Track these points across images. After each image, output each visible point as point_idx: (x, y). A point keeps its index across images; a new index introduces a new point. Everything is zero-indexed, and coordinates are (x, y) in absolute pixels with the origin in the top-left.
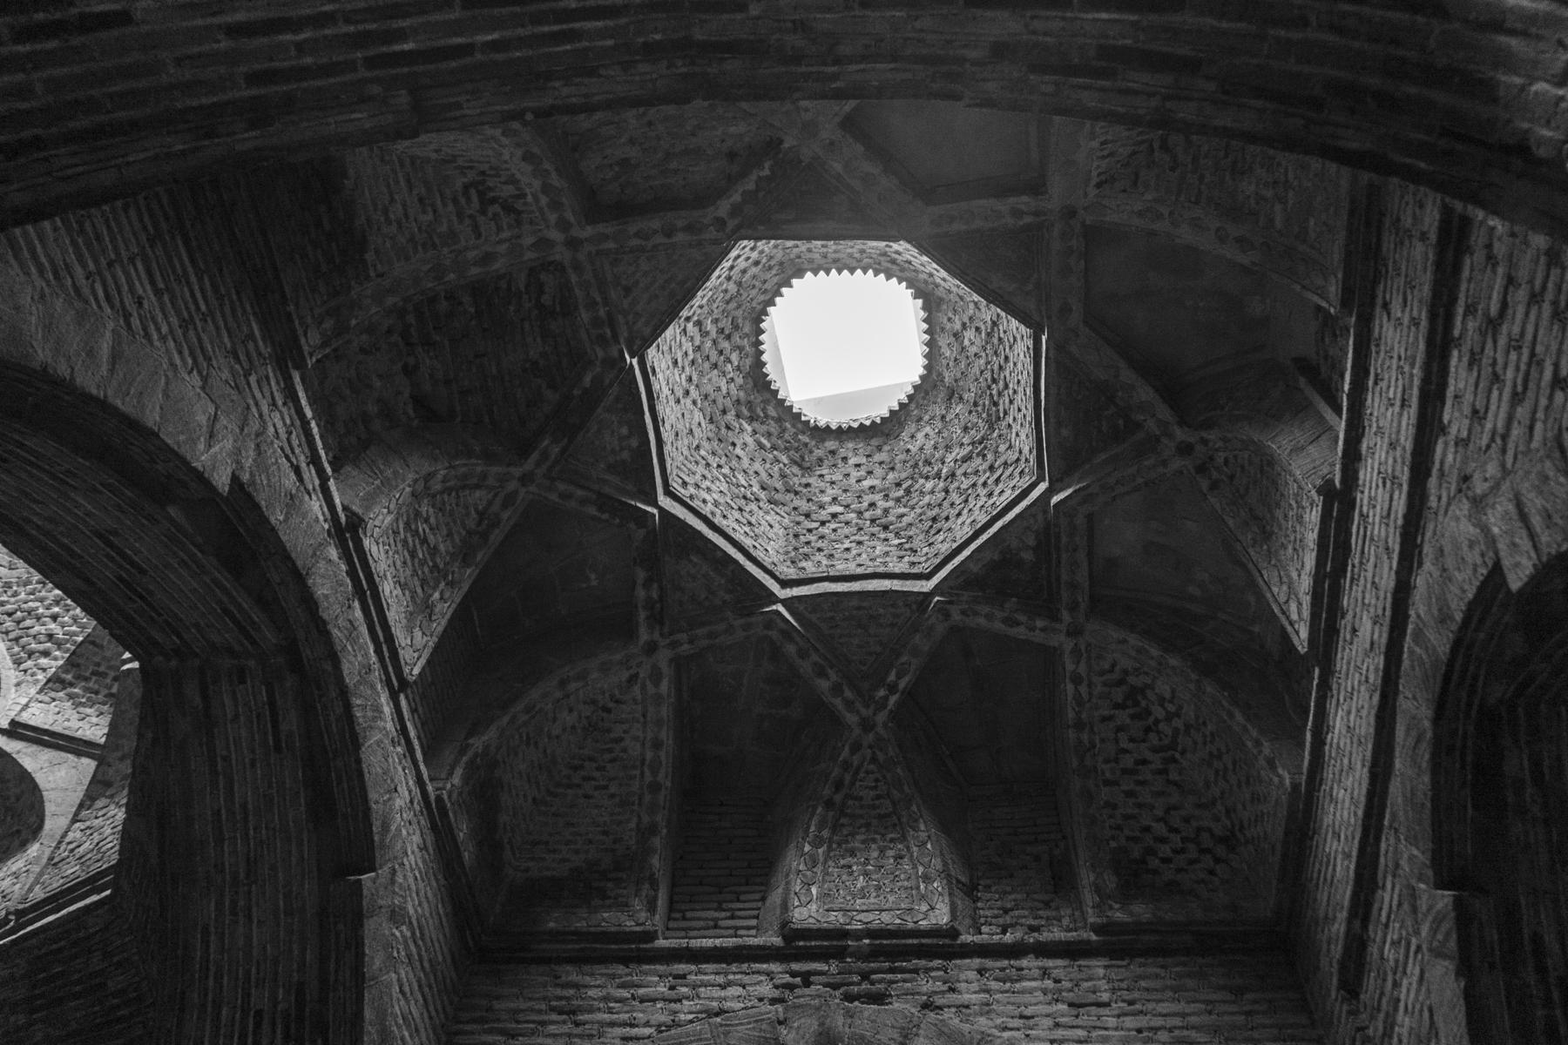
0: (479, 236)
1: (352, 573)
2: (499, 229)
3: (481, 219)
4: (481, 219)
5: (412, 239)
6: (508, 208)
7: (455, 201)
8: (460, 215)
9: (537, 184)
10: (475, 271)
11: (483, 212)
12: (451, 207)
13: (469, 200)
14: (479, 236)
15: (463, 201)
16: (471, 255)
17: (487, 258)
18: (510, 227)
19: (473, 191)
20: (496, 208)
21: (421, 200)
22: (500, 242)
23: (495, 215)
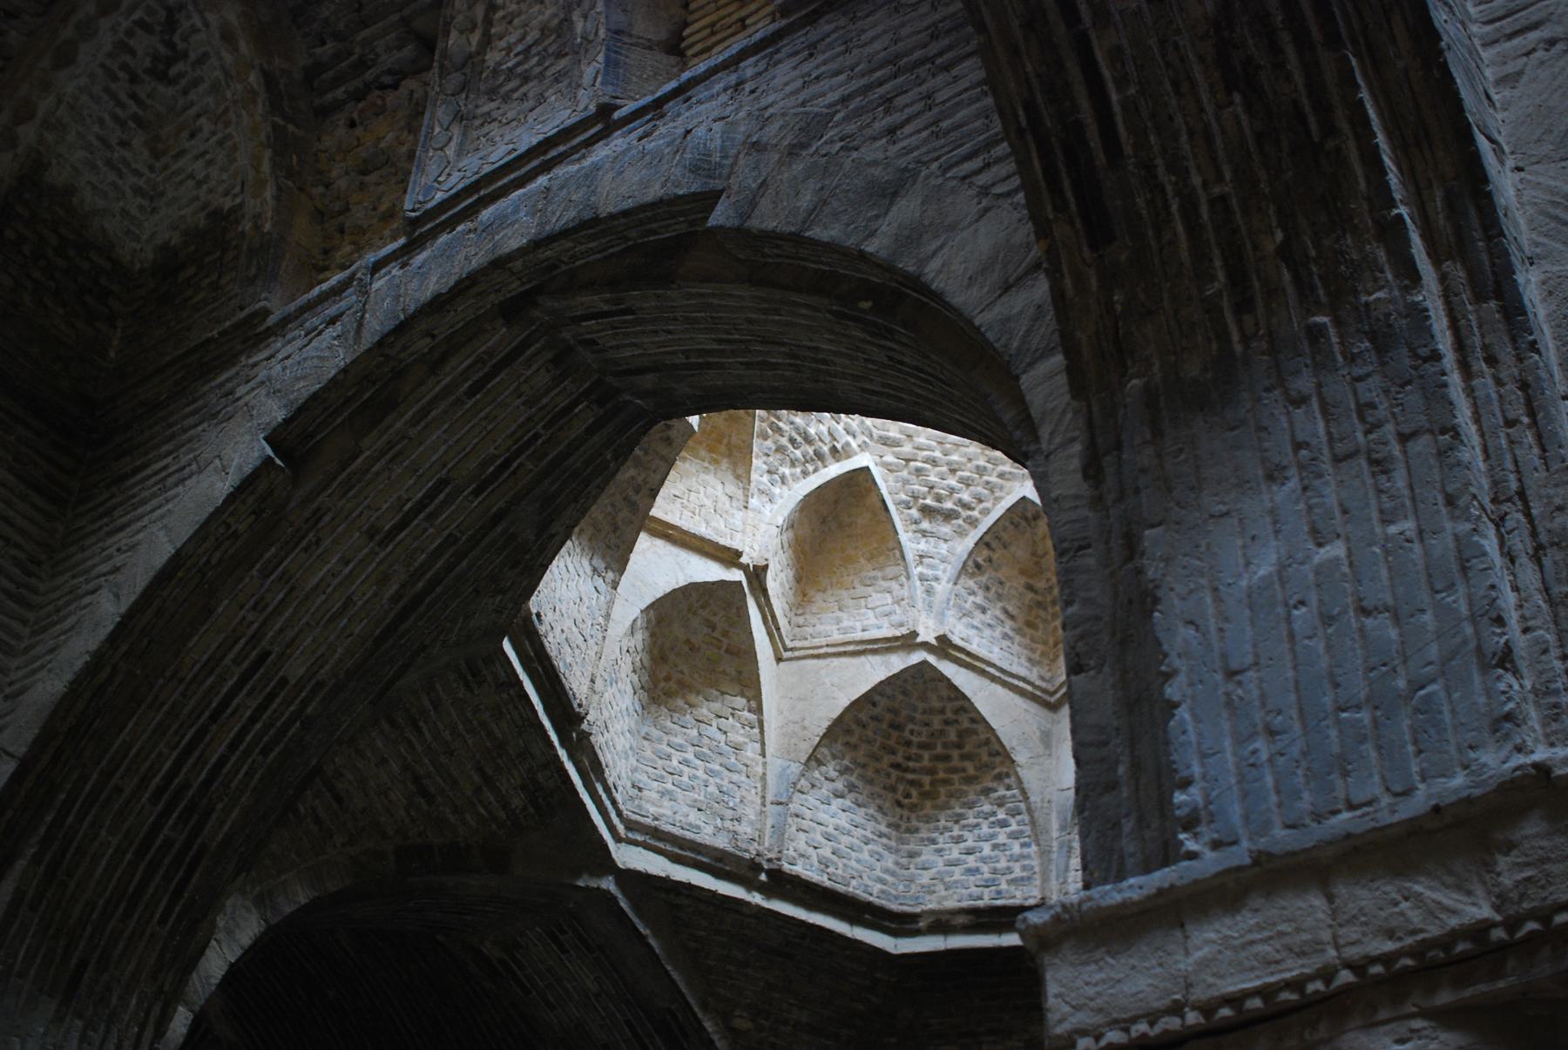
0: (206, 55)
1: (450, 225)
2: (194, 30)
3: (193, 56)
4: (193, 56)
5: (220, 143)
6: (171, 24)
7: (185, 93)
8: (196, 83)
9: (105, 24)
10: (243, 47)
11: (185, 55)
12: (192, 96)
13: (180, 75)
14: (206, 55)
15: (183, 82)
16: (228, 58)
17: (228, 37)
18: (189, 17)
19: (173, 71)
20: (176, 38)
21: (192, 136)
22: (206, 24)
23: (184, 39)
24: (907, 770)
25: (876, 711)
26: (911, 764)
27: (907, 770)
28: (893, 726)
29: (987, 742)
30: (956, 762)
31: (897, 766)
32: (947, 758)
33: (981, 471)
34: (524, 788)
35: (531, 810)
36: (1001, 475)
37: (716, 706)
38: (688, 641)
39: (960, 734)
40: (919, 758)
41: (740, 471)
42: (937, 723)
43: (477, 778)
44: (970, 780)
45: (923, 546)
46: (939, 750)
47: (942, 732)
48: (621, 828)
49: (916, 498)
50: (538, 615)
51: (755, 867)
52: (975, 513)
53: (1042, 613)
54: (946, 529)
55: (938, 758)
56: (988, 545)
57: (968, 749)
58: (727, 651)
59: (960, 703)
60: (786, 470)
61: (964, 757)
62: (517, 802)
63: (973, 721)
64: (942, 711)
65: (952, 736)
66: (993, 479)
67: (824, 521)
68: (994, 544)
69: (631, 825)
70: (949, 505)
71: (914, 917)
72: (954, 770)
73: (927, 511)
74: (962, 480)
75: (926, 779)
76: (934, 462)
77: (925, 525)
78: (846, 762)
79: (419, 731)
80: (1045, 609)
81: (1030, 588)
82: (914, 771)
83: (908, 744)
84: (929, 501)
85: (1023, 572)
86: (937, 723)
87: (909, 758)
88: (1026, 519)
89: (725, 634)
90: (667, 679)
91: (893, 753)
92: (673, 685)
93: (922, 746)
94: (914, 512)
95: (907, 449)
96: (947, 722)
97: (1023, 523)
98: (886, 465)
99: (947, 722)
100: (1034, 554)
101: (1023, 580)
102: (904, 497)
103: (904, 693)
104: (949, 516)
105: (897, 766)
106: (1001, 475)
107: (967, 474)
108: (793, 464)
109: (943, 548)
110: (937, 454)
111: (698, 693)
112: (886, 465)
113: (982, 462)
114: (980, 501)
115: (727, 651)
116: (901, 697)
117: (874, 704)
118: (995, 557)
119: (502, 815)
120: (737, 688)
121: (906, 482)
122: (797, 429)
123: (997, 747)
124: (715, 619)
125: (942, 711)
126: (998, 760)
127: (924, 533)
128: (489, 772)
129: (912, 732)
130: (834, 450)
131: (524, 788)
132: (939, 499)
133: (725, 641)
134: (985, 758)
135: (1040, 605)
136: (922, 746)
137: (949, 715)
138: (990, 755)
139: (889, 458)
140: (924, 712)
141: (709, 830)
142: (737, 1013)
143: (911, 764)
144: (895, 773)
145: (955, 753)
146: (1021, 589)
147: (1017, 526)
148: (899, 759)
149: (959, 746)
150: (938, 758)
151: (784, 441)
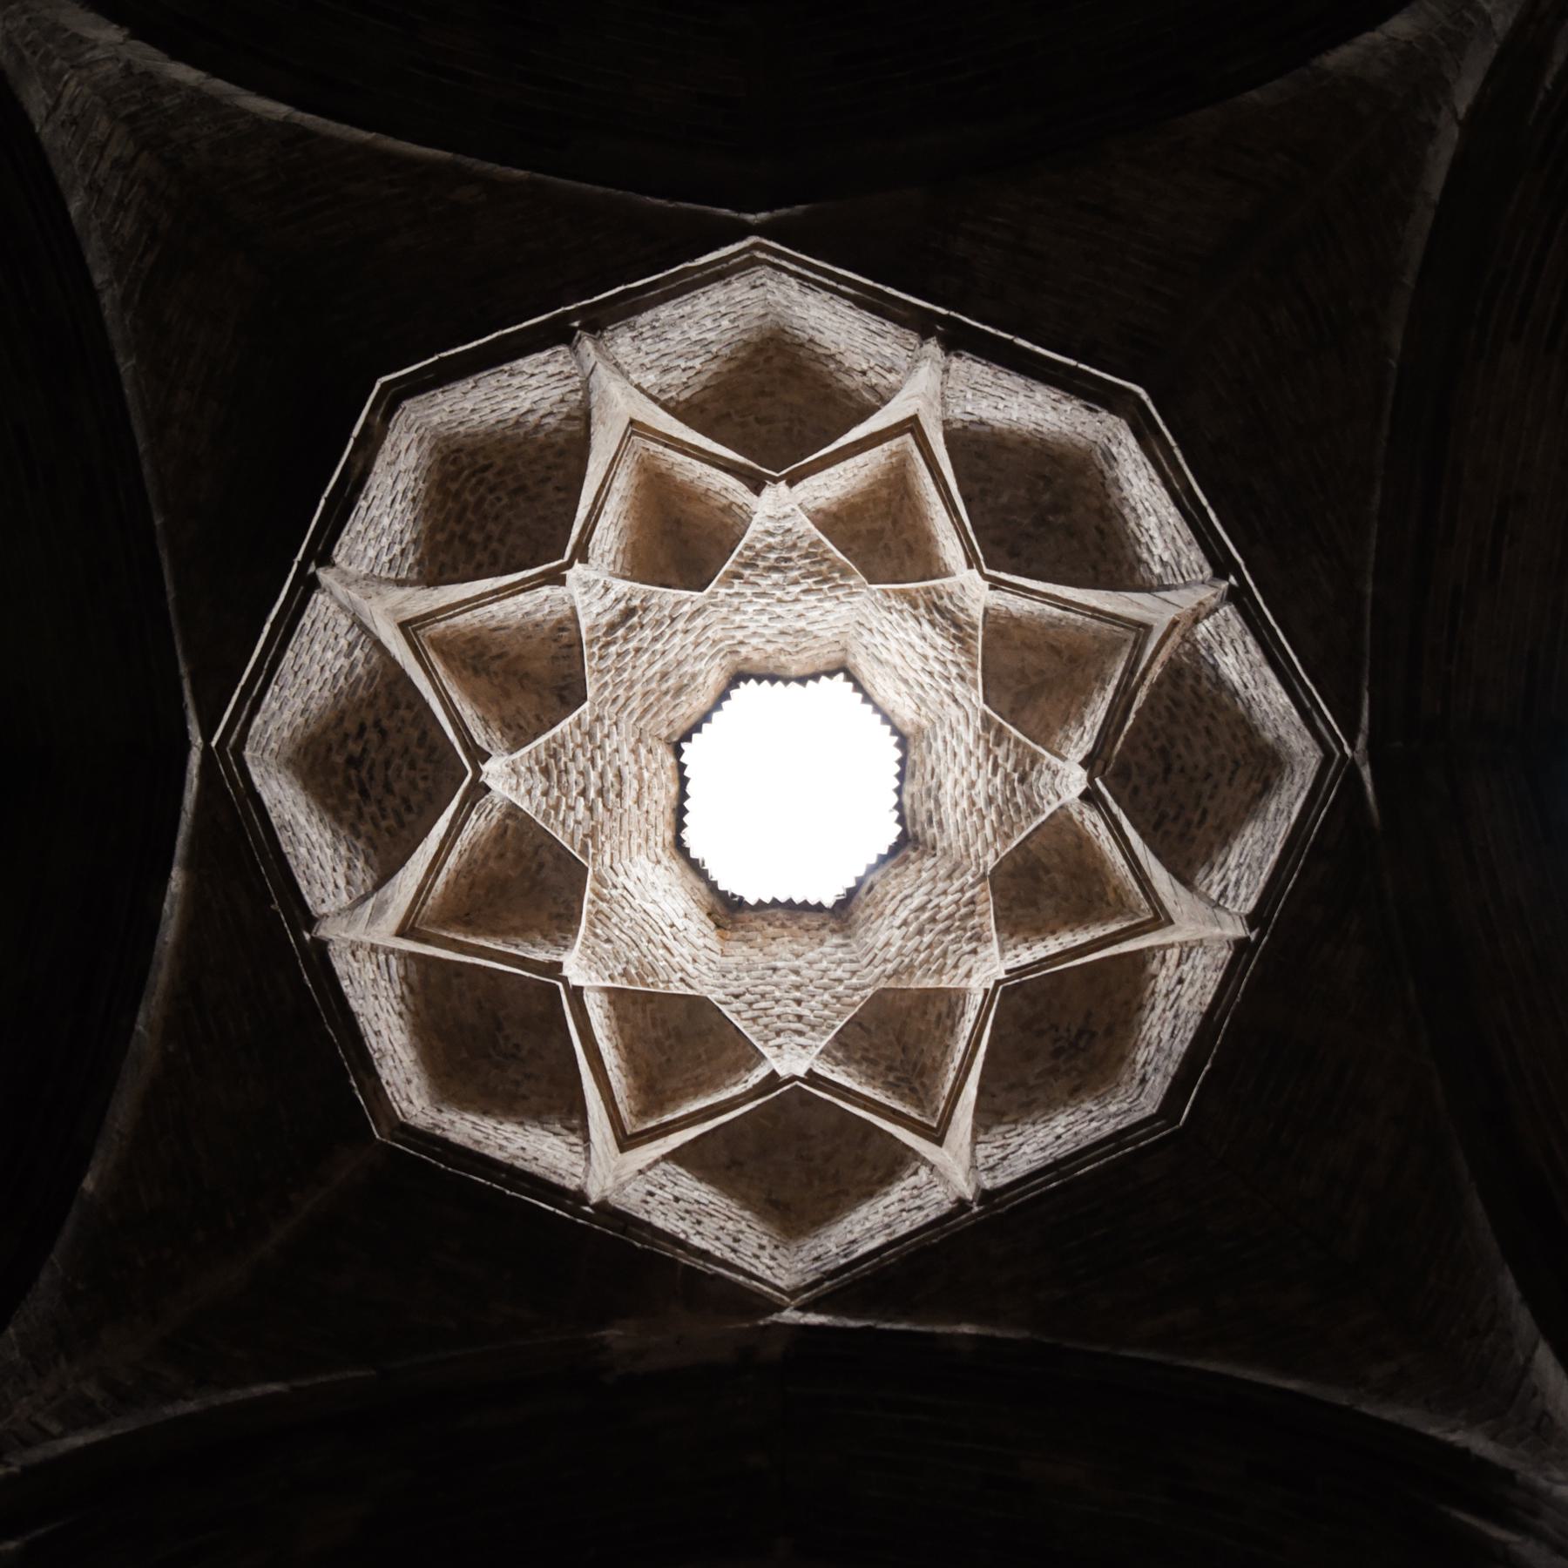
24: (473, 474)
25: (550, 486)
26: (474, 481)
27: (473, 474)
28: (522, 489)
29: (455, 569)
30: (452, 525)
31: (485, 468)
32: (458, 521)
33: (620, 671)
36: (605, 685)
37: (703, 377)
38: (772, 394)
39: (472, 545)
40: (473, 491)
41: (820, 516)
42: (492, 527)
44: (433, 530)
45: (612, 596)
46: (469, 515)
47: (483, 528)
48: (762, 256)
49: (645, 610)
52: (595, 649)
53: (471, 653)
54: (605, 620)
55: (464, 509)
56: (570, 646)
57: (456, 542)
58: (729, 415)
59: (503, 560)
60: (771, 540)
61: (452, 535)
63: (479, 566)
64: (501, 540)
65: (476, 536)
66: (607, 678)
67: (678, 522)
68: (565, 652)
69: (754, 262)
70: (621, 632)
71: (388, 416)
72: (446, 520)
73: (629, 612)
74: (627, 652)
75: (454, 487)
76: (655, 640)
77: (622, 605)
78: (541, 435)
80: (473, 658)
81: (500, 656)
82: (468, 479)
83: (492, 490)
84: (635, 619)
85: (519, 657)
86: (492, 527)
87: (480, 482)
88: (563, 688)
89: (743, 425)
90: (768, 360)
91: (500, 473)
92: (760, 359)
93: (481, 500)
94: (636, 602)
95: (680, 625)
96: (489, 538)
97: (562, 684)
98: (685, 602)
99: (489, 538)
100: (527, 675)
101: (513, 654)
102: (653, 601)
103: (543, 519)
104: (612, 627)
105: (485, 468)
106: (605, 685)
107: (628, 659)
108: (770, 548)
109: (596, 609)
110: (659, 646)
111: (730, 371)
112: (685, 602)
113: (626, 675)
114: (601, 658)
115: (729, 415)
116: (541, 513)
117: (558, 489)
118: (554, 645)
120: (695, 401)
121: (661, 608)
122: (792, 569)
123: (446, 576)
125: (501, 540)
126: (436, 570)
127: (617, 601)
129: (499, 499)
130: (739, 576)
132: (632, 628)
133: (736, 419)
134: (442, 557)
135: (481, 655)
136: (481, 500)
137: (494, 545)
138: (443, 565)
139: (687, 608)
140: (509, 523)
141: (662, 315)
143: (474, 481)
144: (482, 462)
145: (458, 529)
146: (507, 648)
147: (564, 677)
148: (489, 475)
149: (463, 537)
150: (464, 509)
151: (794, 555)
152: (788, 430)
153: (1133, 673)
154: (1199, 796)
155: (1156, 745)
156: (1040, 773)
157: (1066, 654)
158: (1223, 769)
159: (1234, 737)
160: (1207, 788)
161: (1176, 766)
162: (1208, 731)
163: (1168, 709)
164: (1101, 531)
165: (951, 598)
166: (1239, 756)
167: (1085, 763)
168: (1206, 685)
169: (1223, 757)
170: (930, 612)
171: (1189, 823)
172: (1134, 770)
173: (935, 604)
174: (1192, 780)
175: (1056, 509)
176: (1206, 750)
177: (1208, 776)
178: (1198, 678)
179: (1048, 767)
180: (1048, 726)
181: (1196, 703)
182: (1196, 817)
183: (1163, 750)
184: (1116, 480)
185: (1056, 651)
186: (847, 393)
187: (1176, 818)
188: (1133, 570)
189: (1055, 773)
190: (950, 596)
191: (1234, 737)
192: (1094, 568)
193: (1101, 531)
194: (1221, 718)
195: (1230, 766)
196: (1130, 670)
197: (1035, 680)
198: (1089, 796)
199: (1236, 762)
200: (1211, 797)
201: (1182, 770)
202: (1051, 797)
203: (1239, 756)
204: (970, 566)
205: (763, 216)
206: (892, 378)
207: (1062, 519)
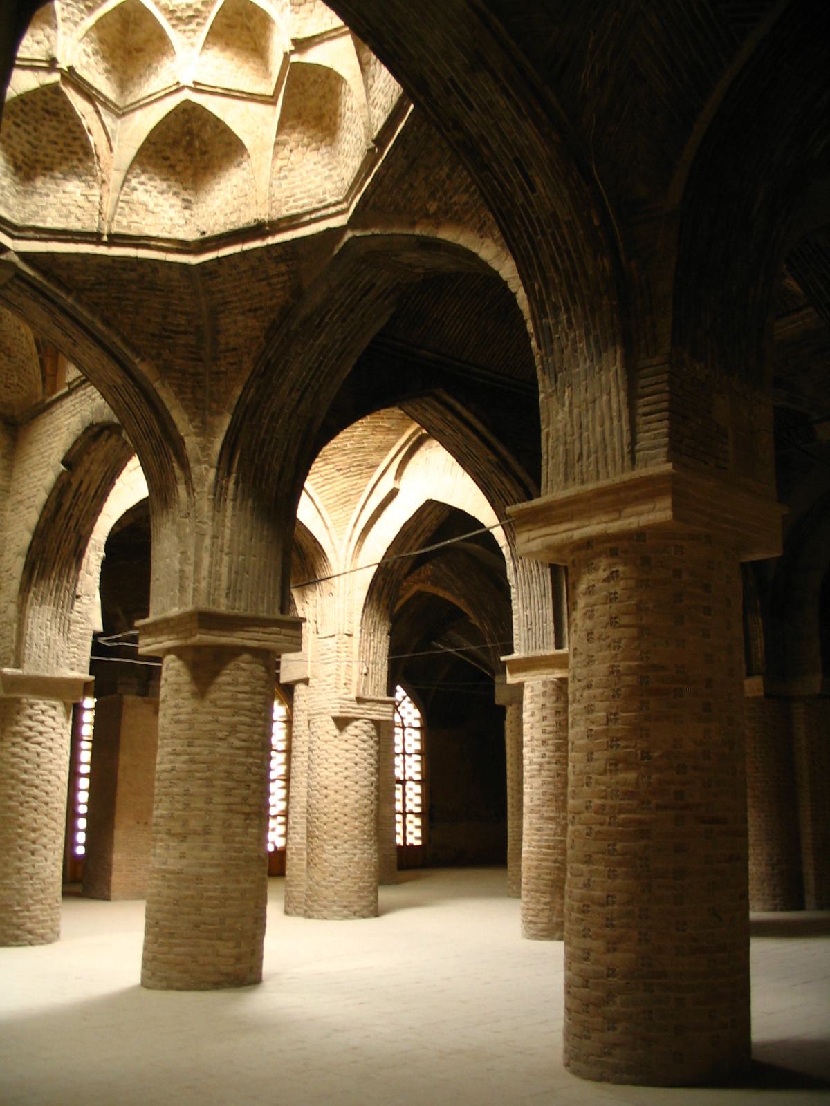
34: (277, 263)
35: (290, 263)
43: (264, 283)
48: (344, 206)
50: (204, 233)
51: (371, 151)
62: (283, 268)
69: (346, 199)
79: (231, 302)
89: (319, 76)
119: (286, 277)
124: (312, 79)
128: (263, 276)
131: (277, 263)
142: (428, 206)
152: (303, 84)
153: (104, 104)
154: (28, 124)
155: (62, 113)
156: (81, 11)
157: (134, 53)
158: (36, 138)
159: (46, 155)
160: (30, 129)
161: (47, 116)
162: (56, 143)
163: (75, 132)
164: (166, 159)
165: (194, 31)
166: (38, 151)
167: (71, 69)
168: (75, 163)
169: (41, 141)
170: (197, 10)
171: (17, 116)
172: (54, 96)
173: (197, 17)
174: (37, 122)
175: (190, 144)
176: (47, 135)
177: (35, 130)
178: (80, 160)
179: (82, 19)
180: (104, 27)
181: (71, 149)
182: (18, 121)
183: (56, 114)
184: (176, 194)
185: (140, 50)
186: (293, 128)
187: (22, 110)
188: (141, 164)
189: (76, 24)
190: (194, 31)
191: (46, 155)
192: (154, 144)
193: (166, 159)
194: (58, 155)
195: (36, 143)
196: (106, 103)
197: (132, 26)
198: (52, 64)
199: (36, 147)
200: (25, 130)
201: (44, 118)
202: (66, 14)
203: (38, 151)
204: (195, 83)
205: (346, 238)
206: (279, 163)
207: (184, 143)
